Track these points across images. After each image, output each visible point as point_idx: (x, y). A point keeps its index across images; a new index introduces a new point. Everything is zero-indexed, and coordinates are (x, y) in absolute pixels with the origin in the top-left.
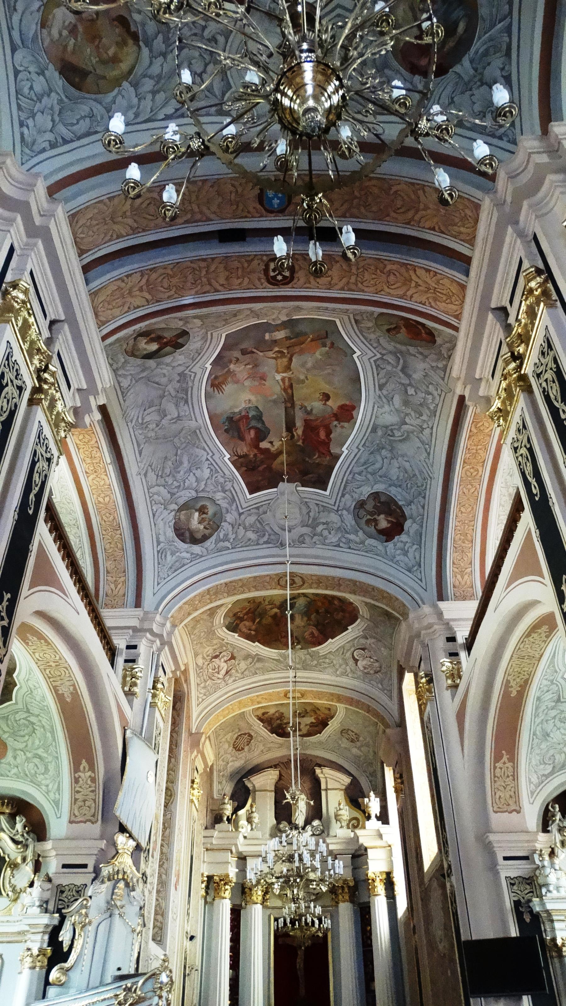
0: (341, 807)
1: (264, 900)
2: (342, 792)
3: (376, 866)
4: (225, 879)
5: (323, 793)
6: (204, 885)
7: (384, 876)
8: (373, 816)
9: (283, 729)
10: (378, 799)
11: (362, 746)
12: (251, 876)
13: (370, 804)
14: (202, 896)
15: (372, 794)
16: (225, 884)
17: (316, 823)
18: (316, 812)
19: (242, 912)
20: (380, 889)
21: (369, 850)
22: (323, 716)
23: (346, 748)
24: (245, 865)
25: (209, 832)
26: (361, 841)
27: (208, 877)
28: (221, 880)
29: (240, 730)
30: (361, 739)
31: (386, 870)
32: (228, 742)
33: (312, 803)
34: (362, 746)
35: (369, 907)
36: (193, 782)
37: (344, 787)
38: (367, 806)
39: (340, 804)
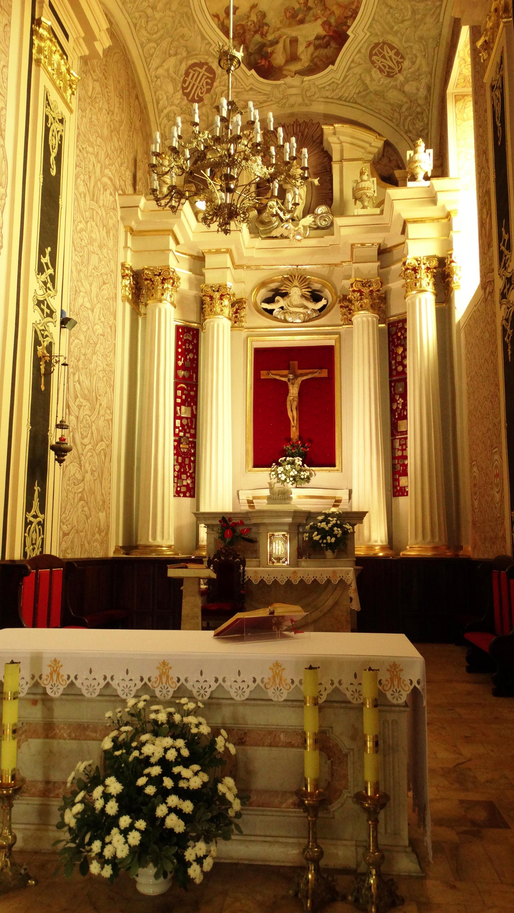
0: (365, 177)
1: (236, 318)
2: (368, 165)
3: (421, 247)
4: (165, 276)
5: (336, 168)
6: (127, 282)
7: (435, 263)
8: (420, 176)
9: (267, 56)
10: (431, 151)
11: (407, 80)
12: (211, 278)
13: (417, 157)
14: (125, 298)
15: (421, 144)
16: (164, 281)
17: (321, 210)
18: (323, 194)
19: (202, 335)
20: (426, 281)
21: (410, 227)
22: (338, 12)
23: (376, 93)
24: (204, 266)
25: (130, 200)
26: (398, 207)
27: (132, 271)
28: (155, 275)
29: (189, 54)
30: (406, 64)
31: (439, 254)
32: (173, 80)
33: (316, 181)
34: (407, 80)
35: (404, 321)
36: (36, 22)
37: (371, 157)
38: (412, 161)
39: (362, 173)
